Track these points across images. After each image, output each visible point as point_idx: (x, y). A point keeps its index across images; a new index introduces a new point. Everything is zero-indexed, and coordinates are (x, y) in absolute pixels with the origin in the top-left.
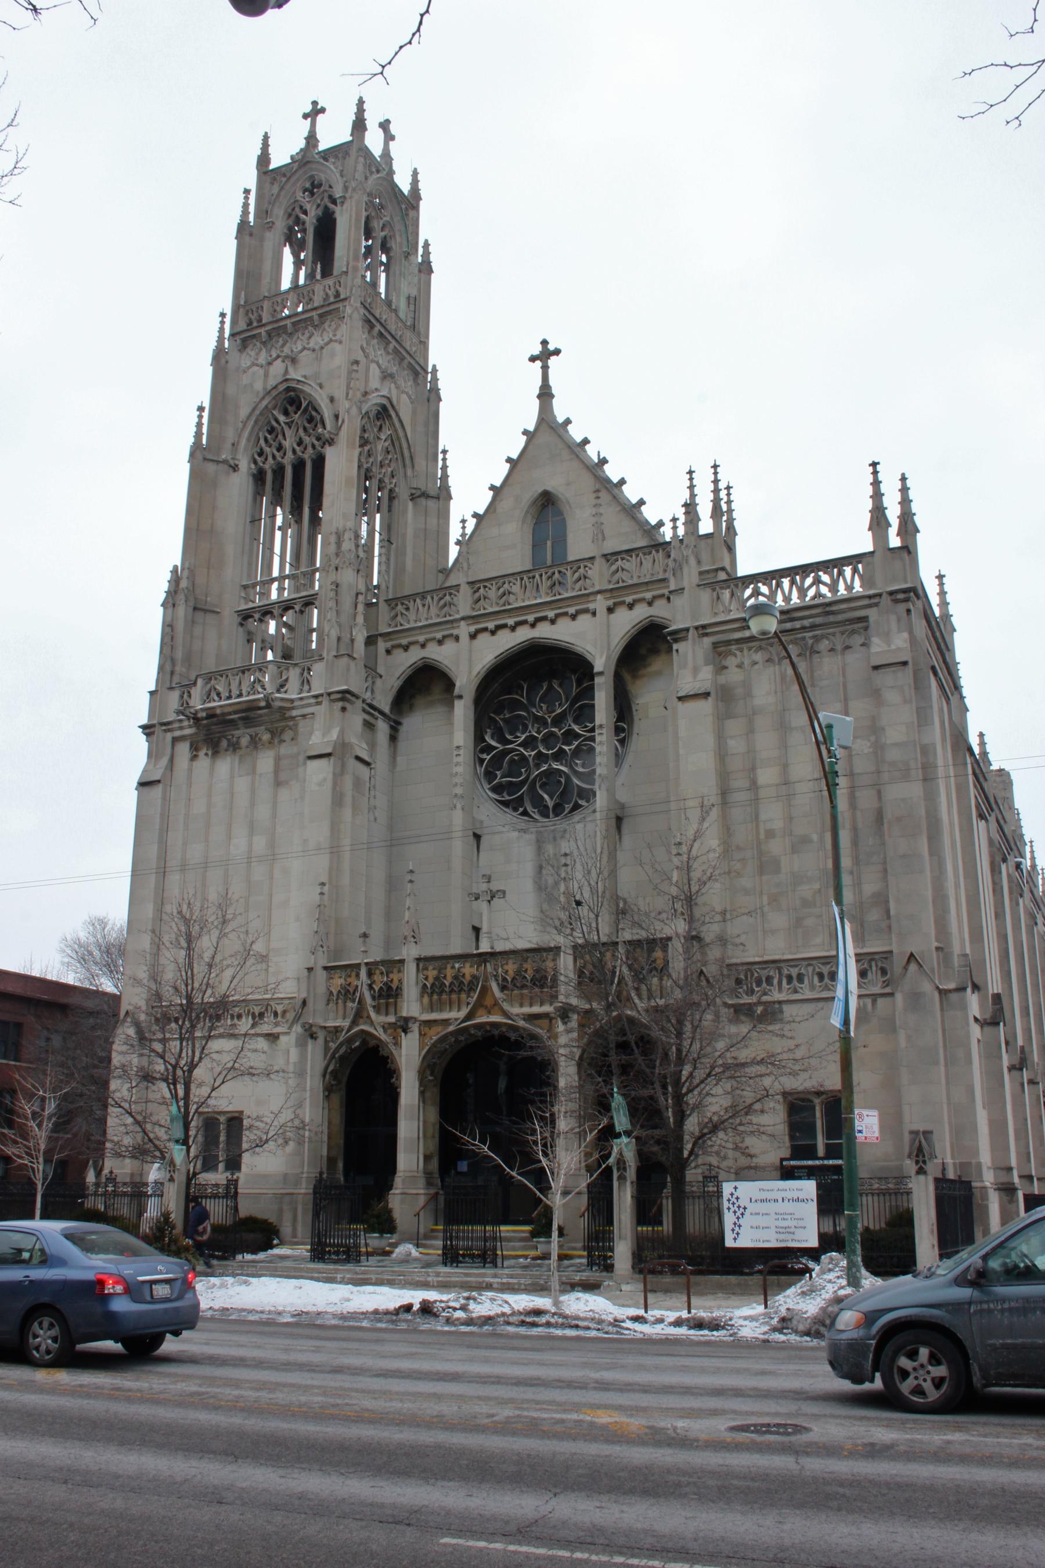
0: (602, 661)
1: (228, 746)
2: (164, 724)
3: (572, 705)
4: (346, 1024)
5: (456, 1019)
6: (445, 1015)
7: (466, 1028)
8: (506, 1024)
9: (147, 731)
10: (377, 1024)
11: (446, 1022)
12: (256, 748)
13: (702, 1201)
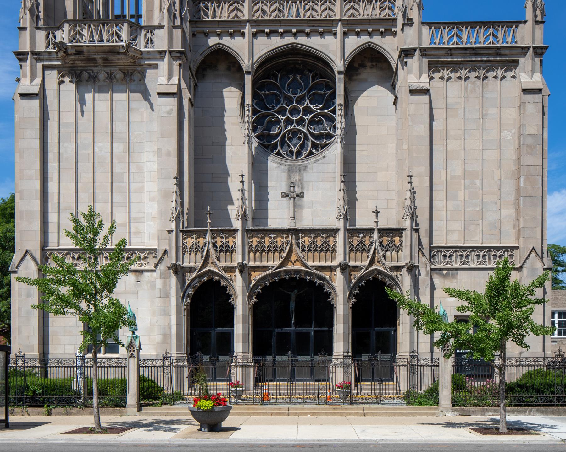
0: (338, 65)
1: (89, 78)
4: (199, 265)
5: (273, 267)
6: (265, 264)
7: (279, 272)
10: (216, 266)
12: (111, 82)
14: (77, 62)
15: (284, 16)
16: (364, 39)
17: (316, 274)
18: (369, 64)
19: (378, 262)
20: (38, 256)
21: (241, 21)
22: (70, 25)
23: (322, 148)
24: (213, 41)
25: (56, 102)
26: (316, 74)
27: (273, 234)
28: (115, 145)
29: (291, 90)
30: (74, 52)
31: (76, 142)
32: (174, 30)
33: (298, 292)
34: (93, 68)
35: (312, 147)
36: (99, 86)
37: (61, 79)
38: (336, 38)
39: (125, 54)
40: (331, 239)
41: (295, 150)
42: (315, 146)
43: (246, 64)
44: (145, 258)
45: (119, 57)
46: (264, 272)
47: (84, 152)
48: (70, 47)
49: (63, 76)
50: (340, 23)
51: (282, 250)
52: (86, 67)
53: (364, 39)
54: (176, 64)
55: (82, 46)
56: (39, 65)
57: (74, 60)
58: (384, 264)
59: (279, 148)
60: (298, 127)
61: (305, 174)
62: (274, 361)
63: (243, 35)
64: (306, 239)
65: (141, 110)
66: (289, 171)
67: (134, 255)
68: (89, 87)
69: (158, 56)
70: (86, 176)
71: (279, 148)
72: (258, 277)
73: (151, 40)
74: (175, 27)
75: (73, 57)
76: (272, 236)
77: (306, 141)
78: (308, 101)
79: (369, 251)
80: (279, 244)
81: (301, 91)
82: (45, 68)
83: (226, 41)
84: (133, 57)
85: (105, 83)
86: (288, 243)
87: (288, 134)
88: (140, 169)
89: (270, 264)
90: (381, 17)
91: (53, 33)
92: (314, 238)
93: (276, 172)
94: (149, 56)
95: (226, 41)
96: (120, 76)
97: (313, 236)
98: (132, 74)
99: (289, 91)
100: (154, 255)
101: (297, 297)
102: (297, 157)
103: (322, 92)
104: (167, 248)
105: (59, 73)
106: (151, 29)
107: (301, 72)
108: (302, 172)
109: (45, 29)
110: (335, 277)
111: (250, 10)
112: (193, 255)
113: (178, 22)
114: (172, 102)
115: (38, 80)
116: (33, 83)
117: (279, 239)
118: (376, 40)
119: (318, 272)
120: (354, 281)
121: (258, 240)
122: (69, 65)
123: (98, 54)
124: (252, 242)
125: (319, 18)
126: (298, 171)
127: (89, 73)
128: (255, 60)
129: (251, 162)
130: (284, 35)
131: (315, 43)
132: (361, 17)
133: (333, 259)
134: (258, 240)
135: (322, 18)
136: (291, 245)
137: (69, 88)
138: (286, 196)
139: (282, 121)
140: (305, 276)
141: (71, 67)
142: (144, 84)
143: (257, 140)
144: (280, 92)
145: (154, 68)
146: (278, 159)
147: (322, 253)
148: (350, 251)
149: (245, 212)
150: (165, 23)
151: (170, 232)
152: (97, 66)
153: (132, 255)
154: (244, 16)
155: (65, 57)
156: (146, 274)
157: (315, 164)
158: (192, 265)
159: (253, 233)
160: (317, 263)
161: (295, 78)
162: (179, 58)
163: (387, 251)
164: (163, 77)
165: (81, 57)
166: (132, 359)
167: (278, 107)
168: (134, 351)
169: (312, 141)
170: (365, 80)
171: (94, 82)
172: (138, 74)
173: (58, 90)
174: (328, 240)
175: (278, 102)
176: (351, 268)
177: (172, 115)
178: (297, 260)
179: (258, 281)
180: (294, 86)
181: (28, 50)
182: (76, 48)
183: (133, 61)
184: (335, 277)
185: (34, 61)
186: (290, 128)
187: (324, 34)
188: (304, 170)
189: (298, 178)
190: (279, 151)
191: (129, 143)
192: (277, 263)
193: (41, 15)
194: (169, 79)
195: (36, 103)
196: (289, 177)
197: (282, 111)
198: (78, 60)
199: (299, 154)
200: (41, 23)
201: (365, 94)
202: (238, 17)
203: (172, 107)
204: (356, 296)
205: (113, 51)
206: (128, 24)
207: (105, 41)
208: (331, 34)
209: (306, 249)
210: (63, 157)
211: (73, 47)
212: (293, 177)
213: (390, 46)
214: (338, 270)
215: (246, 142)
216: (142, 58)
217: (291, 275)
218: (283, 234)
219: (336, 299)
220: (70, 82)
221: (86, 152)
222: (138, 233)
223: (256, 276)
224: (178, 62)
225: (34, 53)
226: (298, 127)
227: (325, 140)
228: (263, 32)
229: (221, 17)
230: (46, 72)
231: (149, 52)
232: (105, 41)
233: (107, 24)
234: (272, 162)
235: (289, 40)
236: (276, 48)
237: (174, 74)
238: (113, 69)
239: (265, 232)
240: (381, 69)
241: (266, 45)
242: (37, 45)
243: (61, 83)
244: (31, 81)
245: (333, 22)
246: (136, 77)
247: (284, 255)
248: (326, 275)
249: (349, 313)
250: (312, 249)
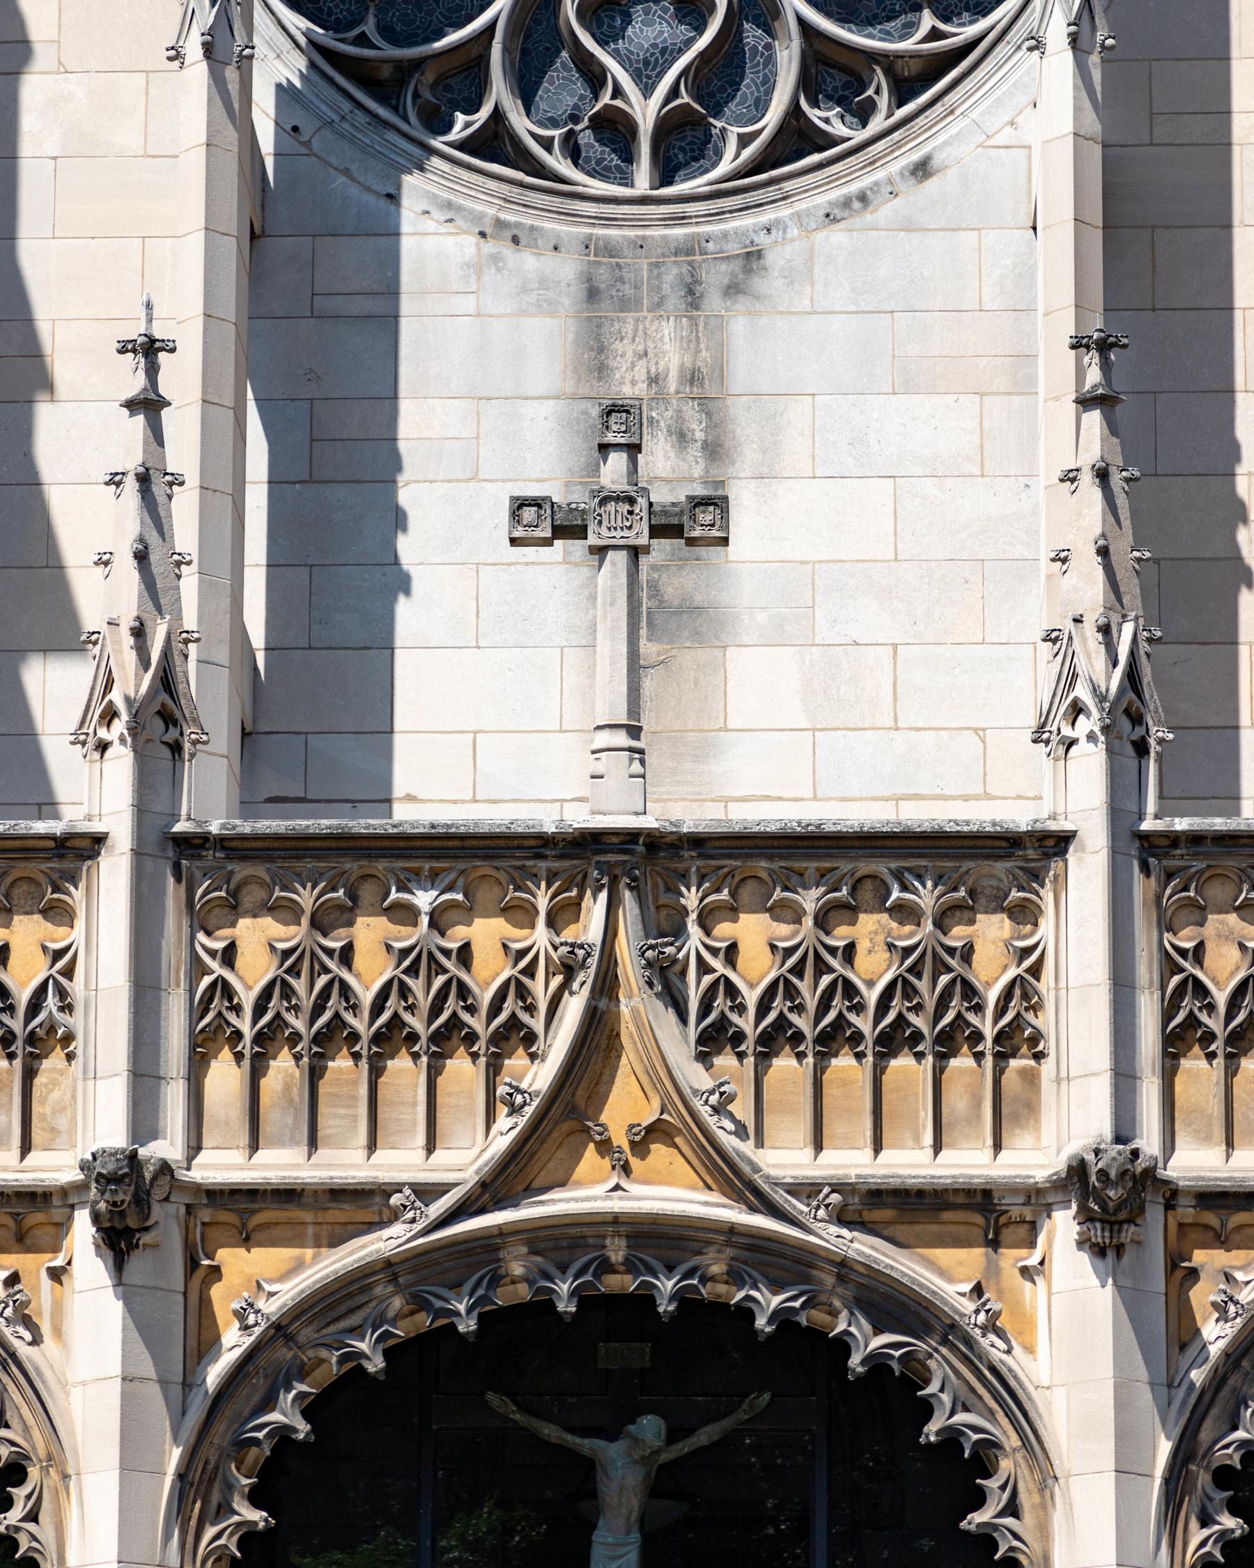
5: (426, 1192)
6: (344, 1163)
7: (486, 1248)
8: (732, 1230)
11: (362, 1204)
17: (843, 1267)
23: (903, 91)
27: (432, 879)
33: (673, 1436)
35: (809, 84)
40: (990, 933)
41: (646, 112)
42: (834, 75)
46: (334, 1243)
51: (515, 1036)
59: (500, 91)
61: (739, 327)
64: (753, 931)
66: (593, 295)
71: (500, 91)
72: (284, 1295)
76: (424, 899)
77: (752, 34)
80: (488, 975)
86: (569, 970)
89: (400, 1162)
92: (823, 921)
93: (468, 304)
101: (663, 1482)
102: (666, 173)
108: (714, 302)
110: (1034, 1295)
117: (486, 933)
119: (862, 1247)
121: (291, 935)
124: (229, 956)
126: (675, 300)
129: (232, 219)
134: (291, 935)
136: (607, 984)
140: (735, 1277)
143: (297, 22)
147: (902, 1063)
148: (1177, 1042)
157: (836, 237)
159: (241, 871)
160: (850, 1160)
169: (805, 27)
174: (958, 935)
176: (1186, 1211)
178: (657, 1132)
179: (280, 1330)
188: (733, 290)
189: (672, 359)
190: (498, 115)
192: (468, 1155)
196: (595, 356)
199: (682, 143)
209: (745, 1023)
212: (624, 350)
214: (1063, 1226)
215: (193, 48)
217: (606, 1267)
219: (1045, 1506)
223: (264, 1282)
227: (928, 20)
239: (352, 867)
247: (539, 1076)
248: (944, 1274)
250: (809, 1023)
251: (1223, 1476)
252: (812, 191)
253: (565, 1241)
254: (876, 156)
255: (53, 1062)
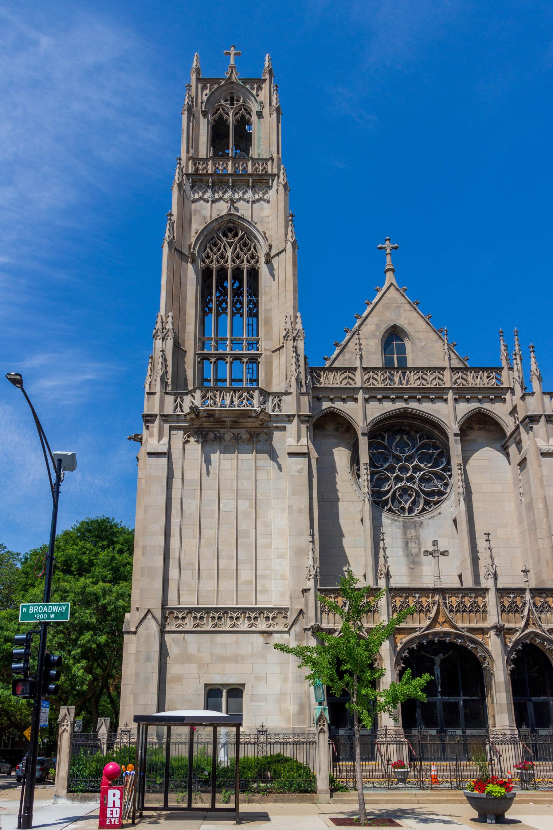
2: (164, 416)
3: (417, 451)
8: (455, 633)
9: (164, 418)
13: (256, 746)
14: (205, 424)
15: (395, 384)
16: (475, 405)
17: (468, 637)
18: (476, 427)
19: (534, 624)
20: (159, 615)
21: (354, 388)
22: (202, 392)
24: (326, 405)
25: (181, 460)
26: (423, 435)
27: (418, 593)
28: (240, 502)
29: (398, 449)
30: (205, 414)
31: (200, 499)
32: (301, 397)
33: (444, 656)
34: (219, 430)
35: (424, 504)
36: (225, 446)
37: (187, 439)
38: (447, 403)
39: (256, 417)
40: (480, 599)
41: (407, 506)
43: (361, 426)
44: (274, 618)
45: (249, 420)
46: (410, 634)
47: (208, 508)
48: (202, 411)
49: (189, 436)
50: (451, 391)
51: (428, 611)
52: (213, 428)
53: (475, 405)
54: (304, 427)
55: (215, 410)
56: (167, 426)
57: (204, 422)
58: (540, 626)
60: (409, 484)
61: (421, 530)
62: (464, 735)
63: (356, 400)
64: (453, 599)
65: (267, 468)
66: (404, 527)
67: (262, 615)
68: (215, 446)
69: (287, 419)
70: (209, 532)
72: (405, 640)
73: (279, 406)
74: (302, 394)
75: (203, 419)
76: (417, 595)
77: (417, 498)
78: (416, 460)
79: (522, 612)
80: (425, 605)
81: (408, 450)
82: (172, 428)
83: (339, 405)
84: (262, 420)
85: (231, 443)
86: (434, 603)
87: (399, 491)
88: (267, 525)
89: (416, 625)
90: (490, 386)
91: (180, 398)
92: (462, 598)
93: (390, 528)
94: (277, 419)
95: (339, 405)
96: (246, 436)
97: (460, 596)
98: (258, 435)
99: (396, 450)
100: (283, 615)
101: (442, 661)
103: (431, 451)
104: (303, 608)
105: (185, 434)
106: (278, 395)
107: (408, 433)
108: (418, 528)
109: (174, 394)
110: (489, 640)
111: (362, 378)
112: (331, 615)
113: (304, 390)
114: (303, 462)
115: (165, 440)
116: (161, 442)
117: (424, 599)
118: (487, 406)
119: (469, 635)
120: (510, 645)
121: (402, 600)
122: (196, 426)
123: (229, 417)
124: (395, 602)
125: (429, 386)
126: (413, 528)
127: (215, 434)
128: (368, 422)
130: (396, 400)
131: (426, 407)
132: (470, 386)
133: (485, 620)
134: (402, 600)
135: (432, 386)
136: (439, 605)
137: (195, 448)
138: (430, 554)
139: (392, 478)
140: (455, 638)
141: (198, 428)
142: (271, 444)
144: (388, 451)
145: (281, 430)
146: (390, 516)
147: (465, 614)
148: (502, 612)
149: (388, 571)
150: (293, 390)
151: (305, 591)
152: (224, 428)
153: (259, 614)
154: (355, 383)
155: (195, 419)
156: (275, 635)
157: (431, 521)
158: (331, 626)
159: (396, 592)
160: (467, 625)
161: (401, 439)
162: (307, 421)
163: (541, 612)
164: (291, 438)
165: (211, 419)
166: (322, 735)
167: (387, 465)
168: (324, 725)
170: (474, 441)
171: (220, 442)
172: (265, 436)
173: (184, 449)
174: (476, 600)
175: (386, 460)
176: (505, 631)
177: (303, 474)
178: (445, 622)
179: (405, 644)
180: (402, 446)
181: (156, 411)
182: (209, 412)
183: (261, 423)
184: (489, 640)
185: (162, 422)
186: (399, 485)
187: (435, 400)
188: (420, 526)
189: (414, 534)
190: (390, 507)
191: (256, 499)
192: (425, 624)
193: (170, 381)
194: (298, 440)
195: (164, 460)
196: (405, 534)
197: (391, 469)
198: (207, 422)
199: (411, 510)
200: (169, 389)
201: (476, 454)
202: (350, 384)
203: (302, 466)
204: (514, 661)
205: (245, 415)
206: (259, 391)
207: (236, 406)
208: (442, 400)
209: (454, 609)
210: (186, 513)
211: (205, 410)
212: (408, 533)
213: (499, 410)
214: (492, 632)
216: (270, 421)
217: (440, 637)
218: (428, 593)
219: (493, 664)
220: (195, 441)
221: (211, 508)
222: (265, 591)
223: (402, 639)
224: (305, 425)
225: (162, 416)
226: (409, 484)
227: (437, 497)
228: (375, 397)
229: (325, 384)
230: (172, 432)
231: (277, 416)
232: (236, 406)
233: (239, 391)
234: (386, 519)
235: (400, 405)
236: (388, 412)
237: (302, 436)
238: (239, 430)
239: (409, 592)
240: (489, 431)
241: (378, 409)
242: (165, 408)
243: (186, 442)
244: (159, 441)
245: (445, 390)
246: (263, 437)
247: (432, 615)
248: (479, 638)
249: (509, 679)
250: (461, 610)
251: (511, 660)
252: (426, 516)
253: (436, 634)
254: (434, 511)
255: (376, 613)
